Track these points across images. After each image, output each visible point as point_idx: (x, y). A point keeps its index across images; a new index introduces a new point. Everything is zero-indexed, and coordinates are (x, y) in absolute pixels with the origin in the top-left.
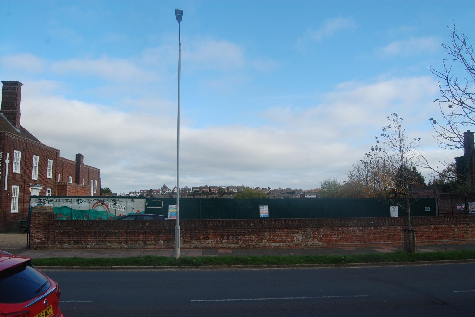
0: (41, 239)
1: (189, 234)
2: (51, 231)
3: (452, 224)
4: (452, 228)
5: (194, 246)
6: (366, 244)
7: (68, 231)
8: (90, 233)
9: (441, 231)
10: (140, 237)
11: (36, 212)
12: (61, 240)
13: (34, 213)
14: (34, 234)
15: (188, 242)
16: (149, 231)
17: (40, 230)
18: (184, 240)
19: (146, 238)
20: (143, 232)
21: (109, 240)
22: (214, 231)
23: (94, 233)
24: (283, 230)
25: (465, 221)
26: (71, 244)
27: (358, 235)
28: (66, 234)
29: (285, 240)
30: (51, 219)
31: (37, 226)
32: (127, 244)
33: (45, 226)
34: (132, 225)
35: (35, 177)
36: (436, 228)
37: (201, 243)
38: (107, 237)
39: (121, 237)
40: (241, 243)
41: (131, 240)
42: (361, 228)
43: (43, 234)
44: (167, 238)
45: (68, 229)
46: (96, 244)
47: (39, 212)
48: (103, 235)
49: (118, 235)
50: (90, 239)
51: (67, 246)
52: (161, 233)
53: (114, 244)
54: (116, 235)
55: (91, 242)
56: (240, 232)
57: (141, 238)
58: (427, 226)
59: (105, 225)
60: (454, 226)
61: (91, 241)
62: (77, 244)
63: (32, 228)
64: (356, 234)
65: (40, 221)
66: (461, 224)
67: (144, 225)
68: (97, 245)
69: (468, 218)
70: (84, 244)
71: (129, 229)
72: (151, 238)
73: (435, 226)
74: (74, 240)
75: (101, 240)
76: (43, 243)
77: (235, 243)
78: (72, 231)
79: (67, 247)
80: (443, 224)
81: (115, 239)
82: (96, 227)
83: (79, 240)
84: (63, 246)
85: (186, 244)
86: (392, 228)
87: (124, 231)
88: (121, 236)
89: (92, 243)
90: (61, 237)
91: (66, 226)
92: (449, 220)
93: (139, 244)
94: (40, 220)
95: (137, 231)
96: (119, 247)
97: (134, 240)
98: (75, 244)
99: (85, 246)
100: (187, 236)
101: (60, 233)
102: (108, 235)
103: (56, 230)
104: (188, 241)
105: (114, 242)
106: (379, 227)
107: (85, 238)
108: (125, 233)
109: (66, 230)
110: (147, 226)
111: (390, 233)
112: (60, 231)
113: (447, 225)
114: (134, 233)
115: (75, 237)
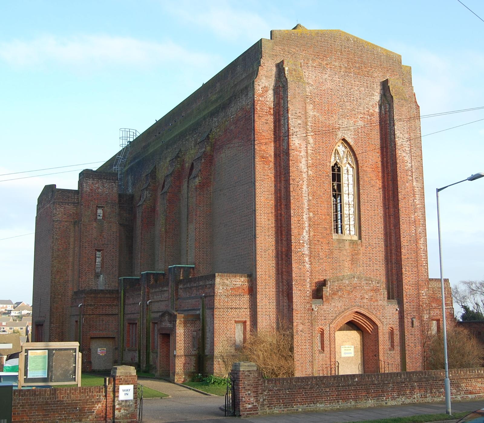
0: (253, 403)
1: (396, 389)
2: (260, 394)
5: (402, 402)
7: (277, 392)
8: (300, 393)
10: (350, 394)
12: (270, 404)
13: (243, 371)
14: (244, 397)
15: (396, 398)
16: (359, 387)
17: (251, 392)
18: (392, 396)
19: (357, 396)
21: (320, 401)
22: (419, 384)
23: (305, 393)
24: (477, 380)
26: (281, 408)
28: (275, 396)
29: (480, 391)
30: (259, 378)
31: (248, 388)
32: (339, 404)
33: (255, 387)
34: (341, 381)
37: (408, 399)
38: (318, 397)
39: (333, 396)
40: (442, 396)
41: (342, 399)
43: (254, 397)
44: (377, 395)
45: (277, 390)
46: (307, 406)
47: (247, 370)
48: (314, 395)
49: (330, 394)
50: (301, 400)
51: (277, 411)
52: (371, 389)
54: (327, 394)
56: (441, 384)
63: (242, 390)
70: (295, 407)
71: (340, 386)
72: (361, 396)
75: (313, 402)
76: (254, 408)
77: (437, 397)
78: (281, 391)
79: (277, 412)
83: (290, 403)
84: (273, 411)
85: (395, 400)
88: (332, 394)
90: (269, 400)
93: (351, 403)
94: (250, 380)
95: (347, 387)
96: (331, 407)
97: (345, 399)
98: (285, 408)
100: (395, 391)
101: (269, 395)
102: (319, 394)
103: (265, 391)
104: (396, 396)
105: (325, 403)
107: (296, 399)
108: (337, 391)
109: (276, 390)
110: (357, 381)
114: (345, 391)
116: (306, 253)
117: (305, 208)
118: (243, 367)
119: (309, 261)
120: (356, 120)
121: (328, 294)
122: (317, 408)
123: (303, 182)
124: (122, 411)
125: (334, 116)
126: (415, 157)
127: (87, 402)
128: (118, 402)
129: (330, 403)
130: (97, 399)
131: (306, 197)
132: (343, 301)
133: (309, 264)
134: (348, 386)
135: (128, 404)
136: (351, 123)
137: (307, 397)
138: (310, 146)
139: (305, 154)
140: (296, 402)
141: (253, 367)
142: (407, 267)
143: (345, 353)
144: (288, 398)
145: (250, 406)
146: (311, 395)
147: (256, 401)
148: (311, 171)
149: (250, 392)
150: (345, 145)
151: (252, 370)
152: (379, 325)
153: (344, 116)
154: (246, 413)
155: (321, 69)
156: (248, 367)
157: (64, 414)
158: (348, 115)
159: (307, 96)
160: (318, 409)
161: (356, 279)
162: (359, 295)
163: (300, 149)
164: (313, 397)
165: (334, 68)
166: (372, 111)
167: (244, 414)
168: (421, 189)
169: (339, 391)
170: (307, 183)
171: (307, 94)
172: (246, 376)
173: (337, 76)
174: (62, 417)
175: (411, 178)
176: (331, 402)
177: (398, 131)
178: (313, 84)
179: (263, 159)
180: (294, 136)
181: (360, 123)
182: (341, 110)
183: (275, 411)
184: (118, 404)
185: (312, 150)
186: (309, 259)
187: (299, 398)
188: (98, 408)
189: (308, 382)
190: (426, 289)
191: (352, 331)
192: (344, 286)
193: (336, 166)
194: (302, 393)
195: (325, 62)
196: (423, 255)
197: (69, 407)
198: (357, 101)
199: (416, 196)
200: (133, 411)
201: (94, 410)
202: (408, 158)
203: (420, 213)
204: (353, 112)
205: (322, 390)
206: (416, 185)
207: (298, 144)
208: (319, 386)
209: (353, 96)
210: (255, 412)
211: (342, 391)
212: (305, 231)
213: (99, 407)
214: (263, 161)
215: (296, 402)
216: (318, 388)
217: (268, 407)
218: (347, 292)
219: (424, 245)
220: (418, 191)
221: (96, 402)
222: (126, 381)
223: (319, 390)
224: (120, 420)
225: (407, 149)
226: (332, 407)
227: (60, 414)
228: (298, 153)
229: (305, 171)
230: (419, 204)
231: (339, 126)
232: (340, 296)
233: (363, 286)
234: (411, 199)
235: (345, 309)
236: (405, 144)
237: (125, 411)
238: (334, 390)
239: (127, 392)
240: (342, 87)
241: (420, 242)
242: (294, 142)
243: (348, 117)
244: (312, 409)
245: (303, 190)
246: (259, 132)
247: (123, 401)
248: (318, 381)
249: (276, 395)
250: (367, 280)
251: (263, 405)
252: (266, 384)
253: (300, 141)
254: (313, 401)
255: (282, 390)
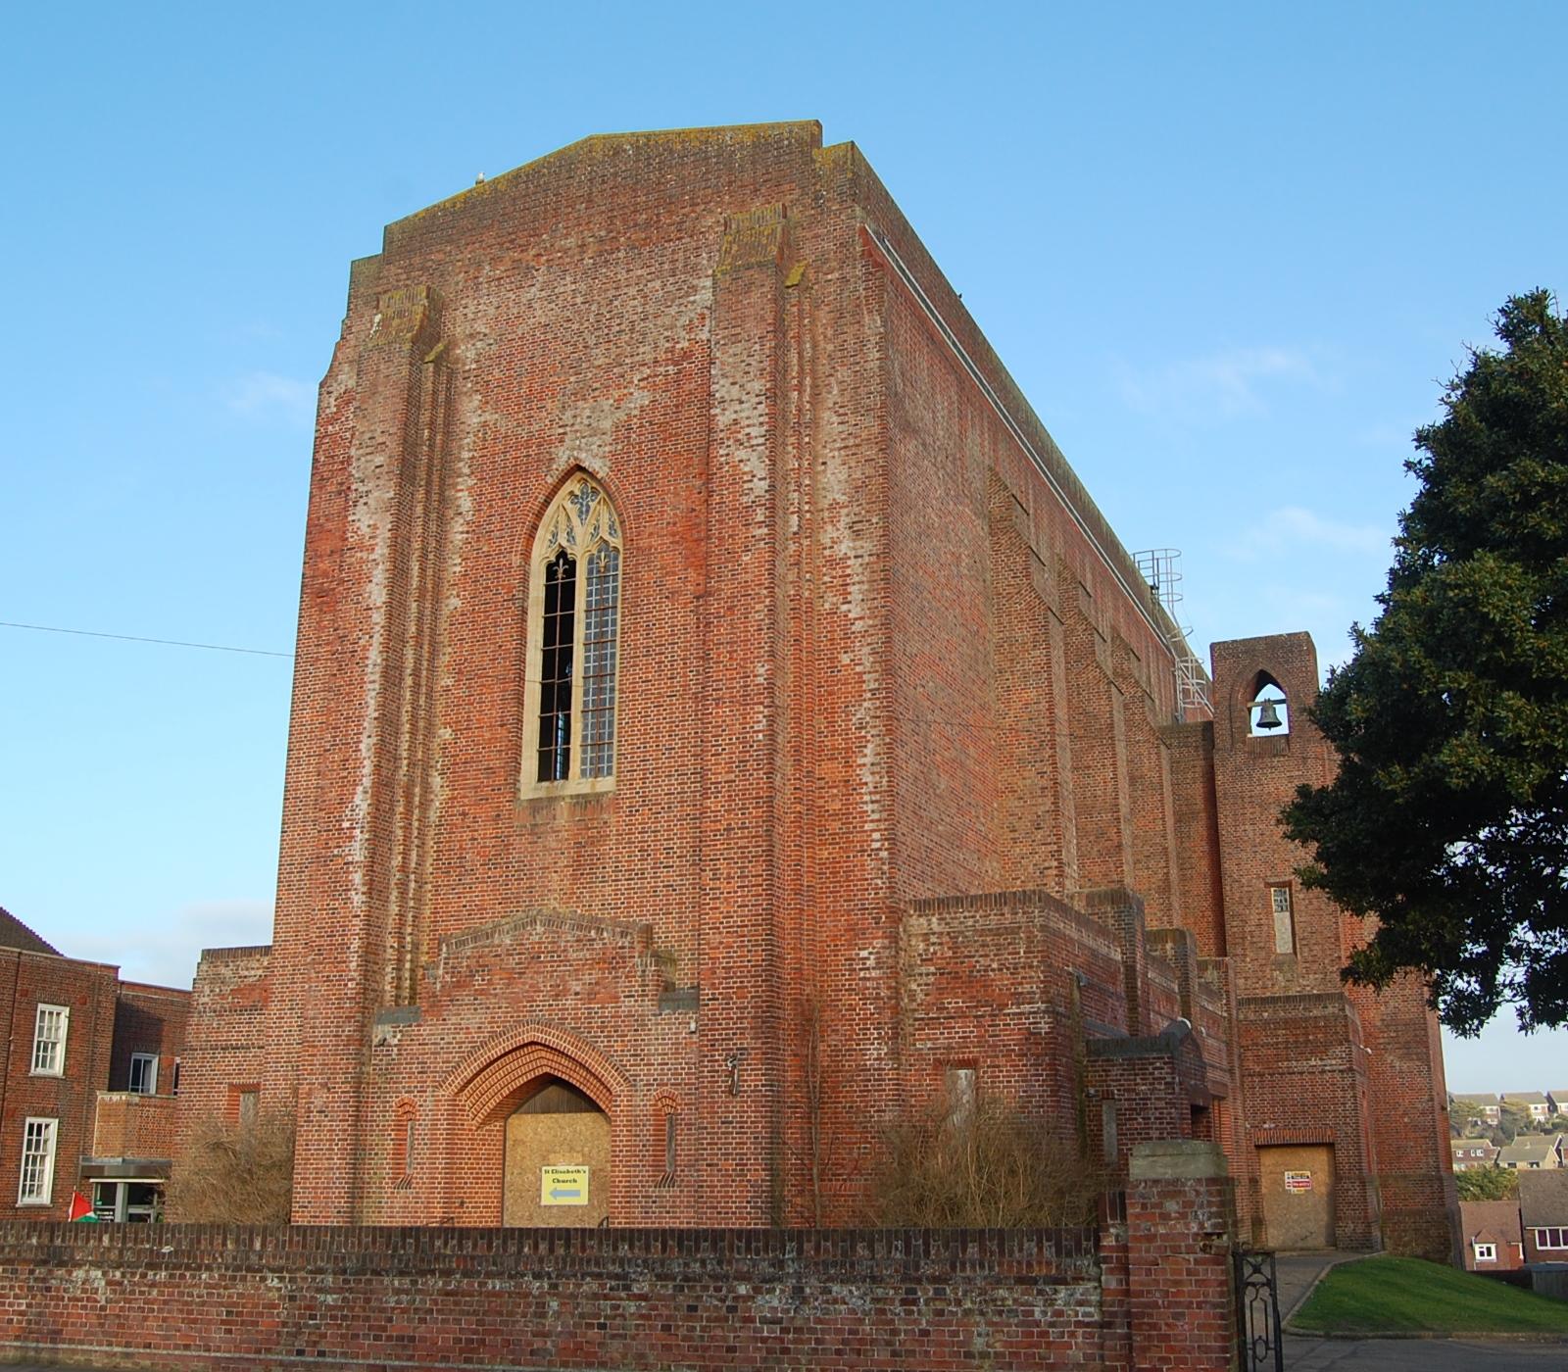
3: (537, 1276)
4: (534, 1297)
6: (127, 1355)
9: (476, 1313)
25: (614, 1263)
27: (103, 1308)
36: (448, 1294)
42: (118, 1274)
58: (407, 1280)
60: (546, 1286)
64: (96, 1301)
66: (583, 1279)
69: (631, 1247)
73: (446, 1284)
80: (489, 1275)
86: (244, 1279)
92: (526, 1250)
106: (188, 1274)
111: (236, 1304)
113: (511, 1277)
116: (357, 858)
117: (367, 719)
119: (364, 884)
120: (626, 391)
121: (438, 986)
123: (371, 637)
125: (549, 405)
126: (854, 450)
131: (374, 682)
132: (488, 1008)
133: (363, 893)
136: (606, 408)
138: (462, 521)
139: (386, 551)
142: (722, 865)
143: (555, 1193)
148: (458, 596)
150: (594, 485)
152: (616, 1089)
153: (579, 395)
155: (519, 278)
158: (598, 385)
159: (466, 375)
161: (539, 929)
162: (546, 985)
163: (372, 542)
165: (560, 258)
166: (687, 344)
168: (873, 559)
170: (381, 640)
171: (467, 368)
173: (568, 279)
175: (766, 530)
177: (722, 382)
178: (487, 331)
179: (319, 600)
180: (360, 507)
181: (641, 398)
182: (572, 379)
185: (468, 532)
186: (364, 875)
190: (878, 943)
191: (584, 1115)
192: (496, 956)
193: (561, 562)
195: (533, 252)
196: (869, 808)
198: (632, 331)
199: (850, 589)
202: (757, 463)
203: (866, 650)
204: (615, 370)
206: (854, 549)
207: (369, 526)
209: (618, 321)
212: (360, 789)
214: (322, 603)
218: (504, 976)
219: (876, 769)
220: (860, 570)
225: (754, 431)
228: (364, 555)
229: (378, 605)
230: (861, 618)
231: (561, 431)
232: (482, 992)
233: (564, 951)
234: (758, 607)
235: (493, 1035)
236: (748, 418)
240: (582, 307)
241: (860, 761)
242: (358, 524)
243: (597, 393)
245: (367, 662)
246: (316, 525)
250: (580, 927)
253: (374, 517)
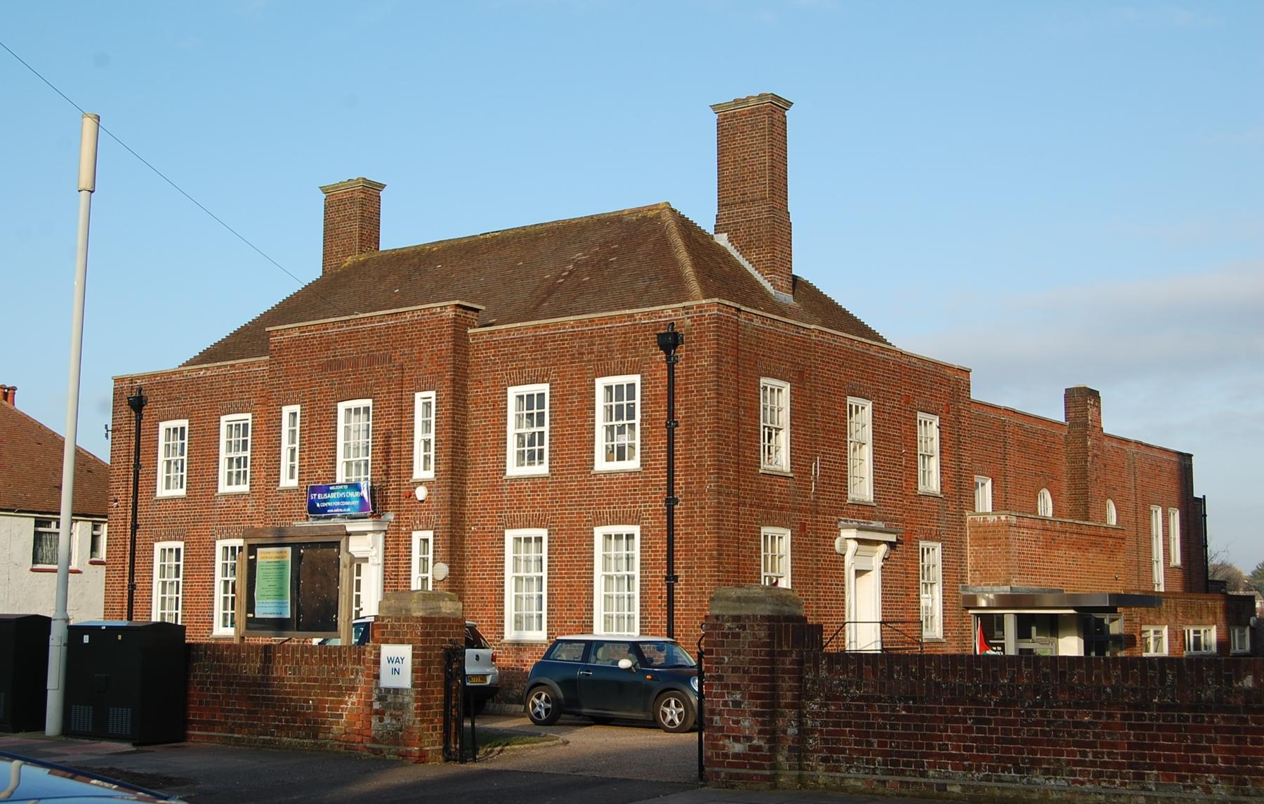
0: (749, 739)
7: (858, 707)
8: (957, 721)
10: (1207, 749)
11: (723, 616)
12: (831, 750)
13: (717, 617)
14: (720, 714)
20: (1222, 724)
21: (1048, 762)
23: (977, 721)
30: (785, 648)
31: (732, 679)
32: (1144, 788)
35: (862, 486)
38: (1039, 743)
43: (754, 714)
45: (861, 698)
46: (987, 778)
48: (1017, 732)
49: (1095, 735)
50: (958, 748)
53: (1075, 782)
54: (1084, 734)
55: (966, 763)
57: (1214, 755)
59: (1025, 681)
61: (963, 758)
62: (902, 773)
65: (741, 657)
67: (1229, 680)
68: (993, 784)
70: (931, 772)
71: (1148, 708)
74: (889, 754)
75: (1010, 760)
76: (756, 757)
79: (859, 784)
81: (1078, 758)
82: (986, 688)
84: (843, 779)
87: (1125, 717)
88: (1108, 739)
89: (969, 768)
90: (828, 733)
91: (851, 685)
93: (1208, 790)
94: (739, 653)
96: (1102, 798)
98: (890, 773)
99: (937, 784)
103: (811, 698)
105: (1073, 773)
108: (1131, 727)
110: (1248, 692)
112: (826, 705)
114: (1178, 729)
115: (891, 736)
118: (720, 604)
122: (1032, 791)
124: (387, 720)
127: (328, 688)
128: (377, 691)
129: (1098, 776)
130: (351, 680)
134: (1192, 709)
135: (401, 700)
137: (985, 739)
140: (940, 756)
141: (752, 605)
144: (900, 736)
145: (738, 748)
146: (1005, 731)
147: (760, 732)
149: (738, 697)
151: (750, 613)
154: (723, 772)
156: (737, 604)
157: (284, 714)
160: (1036, 796)
164: (1014, 741)
167: (718, 774)
169: (1142, 727)
172: (725, 635)
174: (280, 721)
176: (1101, 774)
183: (852, 782)
184: (380, 699)
187: (949, 738)
188: (349, 703)
189: (995, 679)
194: (965, 721)
197: (294, 697)
200: (411, 723)
201: (342, 709)
205: (1060, 715)
208: (1046, 696)
210: (756, 772)
211: (1160, 728)
213: (353, 704)
215: (940, 756)
216: (1036, 705)
217: (824, 760)
221: (346, 690)
222: (397, 634)
223: (1043, 714)
224: (382, 746)
226: (1107, 796)
227: (277, 713)
237: (394, 722)
238: (1117, 720)
239: (397, 666)
244: (1008, 793)
247: (388, 690)
248: (1045, 676)
249: (856, 716)
251: (800, 752)
252: (823, 674)
254: (1017, 759)
255: (879, 699)
